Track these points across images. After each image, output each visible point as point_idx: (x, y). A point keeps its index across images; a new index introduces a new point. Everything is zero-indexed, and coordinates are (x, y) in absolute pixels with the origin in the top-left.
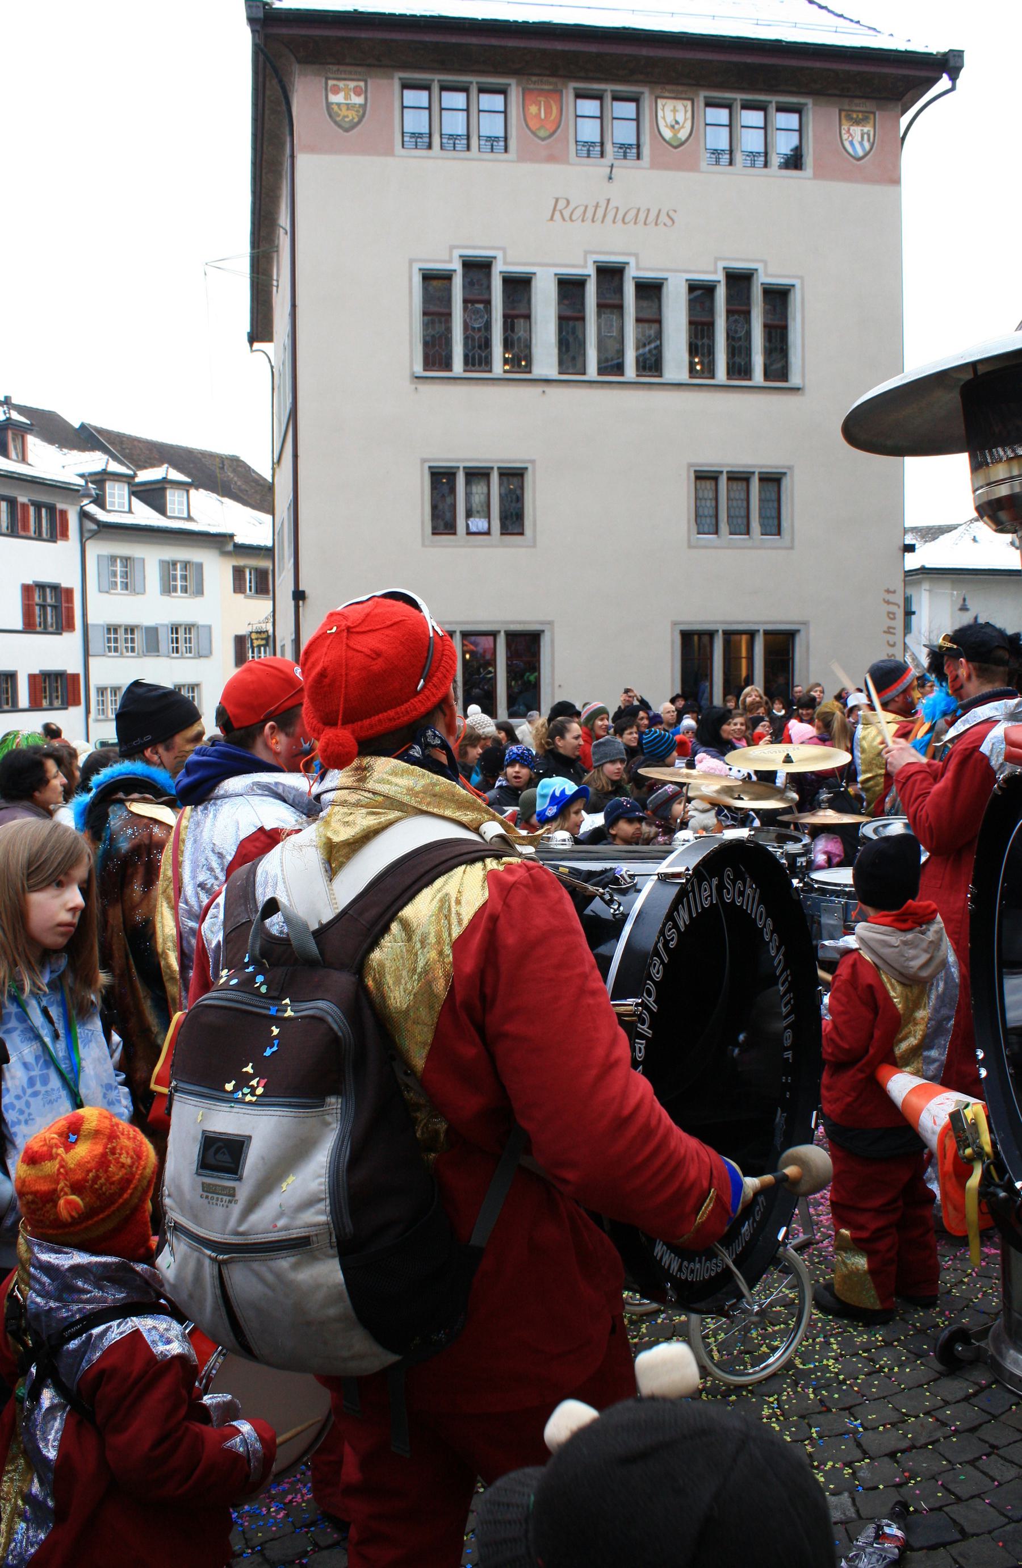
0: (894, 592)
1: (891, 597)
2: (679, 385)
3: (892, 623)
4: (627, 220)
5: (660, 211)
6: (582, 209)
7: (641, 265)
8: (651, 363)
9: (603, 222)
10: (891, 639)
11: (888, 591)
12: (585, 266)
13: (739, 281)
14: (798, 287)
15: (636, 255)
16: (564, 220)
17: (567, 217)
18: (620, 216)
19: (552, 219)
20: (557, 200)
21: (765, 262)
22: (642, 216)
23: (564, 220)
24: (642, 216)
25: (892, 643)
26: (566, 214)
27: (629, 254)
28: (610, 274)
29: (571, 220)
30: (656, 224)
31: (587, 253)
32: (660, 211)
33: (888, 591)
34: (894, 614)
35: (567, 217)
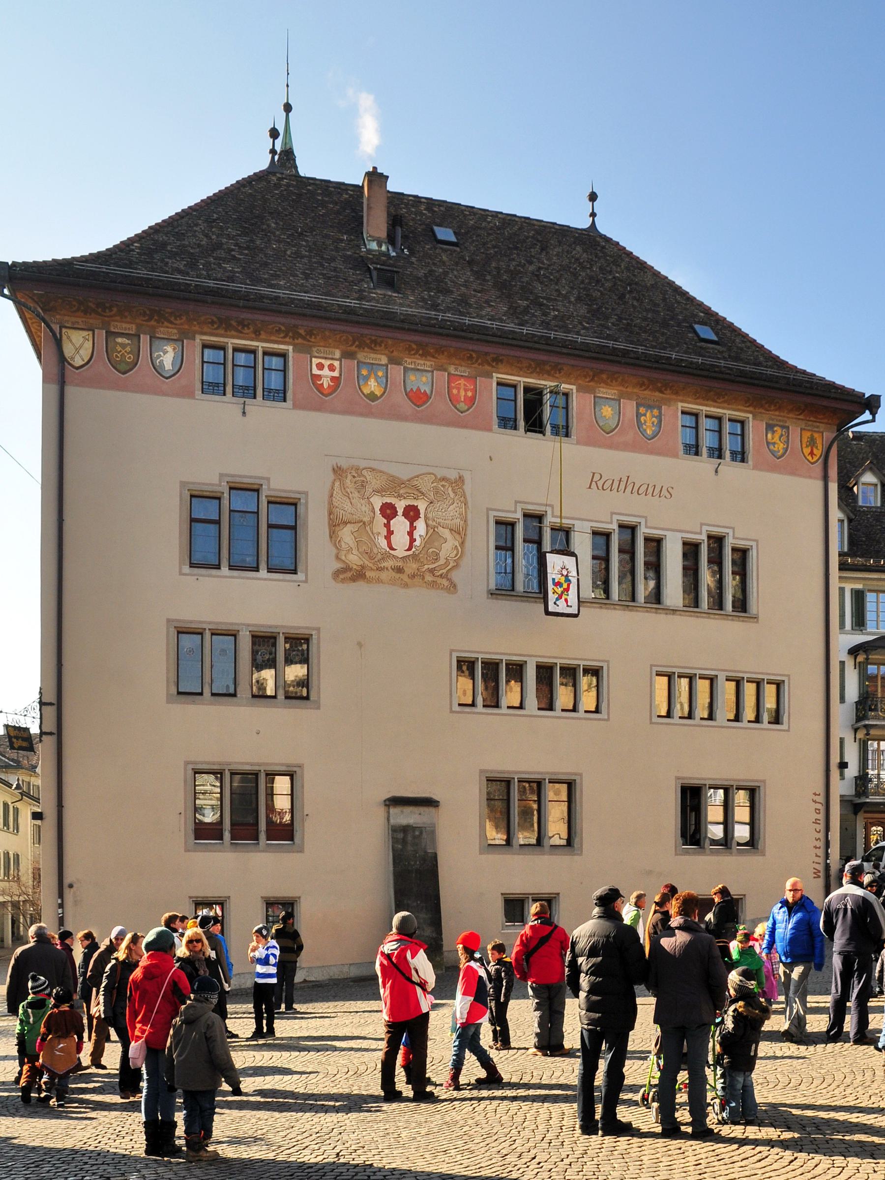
2: (675, 611)
6: (610, 482)
7: (649, 525)
8: (657, 597)
13: (717, 541)
14: (754, 547)
15: (646, 517)
17: (600, 488)
19: (590, 487)
20: (594, 474)
21: (733, 529)
22: (650, 490)
24: (650, 490)
26: (600, 484)
27: (643, 517)
31: (612, 513)
35: (600, 488)
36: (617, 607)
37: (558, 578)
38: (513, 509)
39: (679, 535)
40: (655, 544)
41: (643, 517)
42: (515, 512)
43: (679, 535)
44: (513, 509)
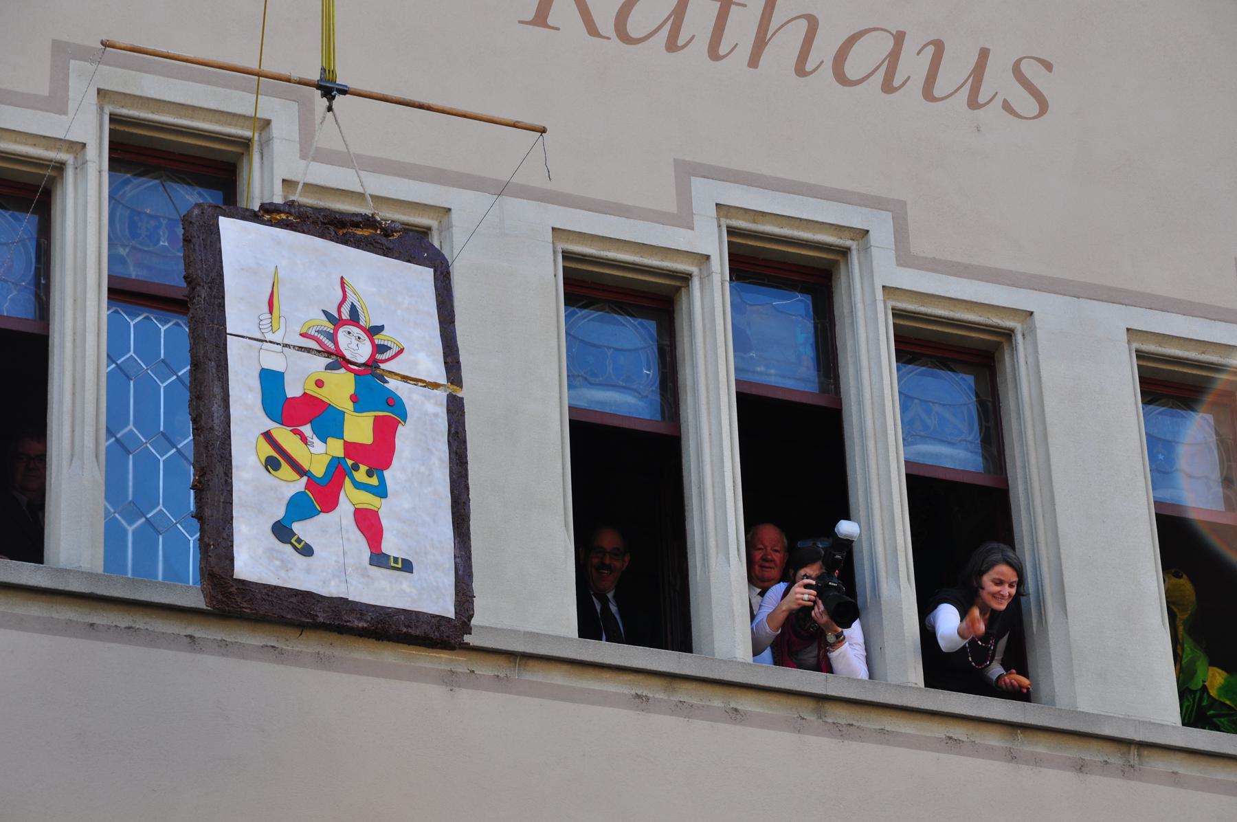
4: (853, 69)
5: (984, 54)
9: (754, 62)
12: (684, 219)
16: (592, 30)
17: (606, 24)
18: (825, 49)
19: (541, 19)
22: (913, 65)
23: (592, 30)
24: (913, 65)
27: (877, 203)
28: (790, 272)
29: (625, 37)
30: (973, 103)
32: (984, 54)
35: (606, 24)
36: (749, 704)
37: (302, 374)
38: (42, 87)
39: (1117, 320)
40: (960, 355)
41: (877, 203)
42: (56, 103)
43: (1117, 320)
44: (42, 87)
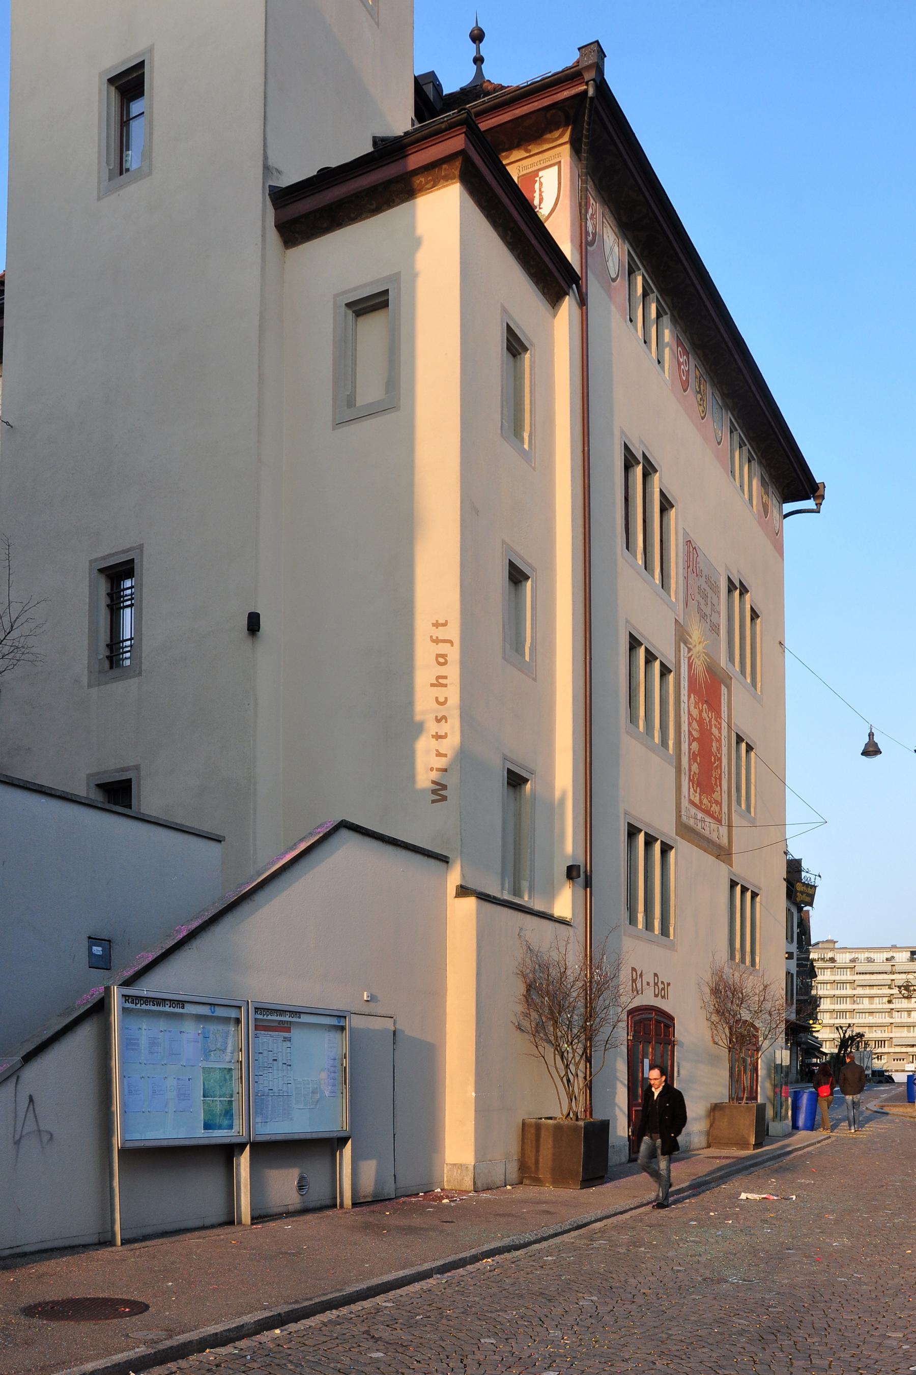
0: (445, 624)
1: (441, 633)
3: (442, 671)
10: (441, 693)
11: (436, 625)
25: (441, 700)
33: (436, 625)
34: (444, 656)
